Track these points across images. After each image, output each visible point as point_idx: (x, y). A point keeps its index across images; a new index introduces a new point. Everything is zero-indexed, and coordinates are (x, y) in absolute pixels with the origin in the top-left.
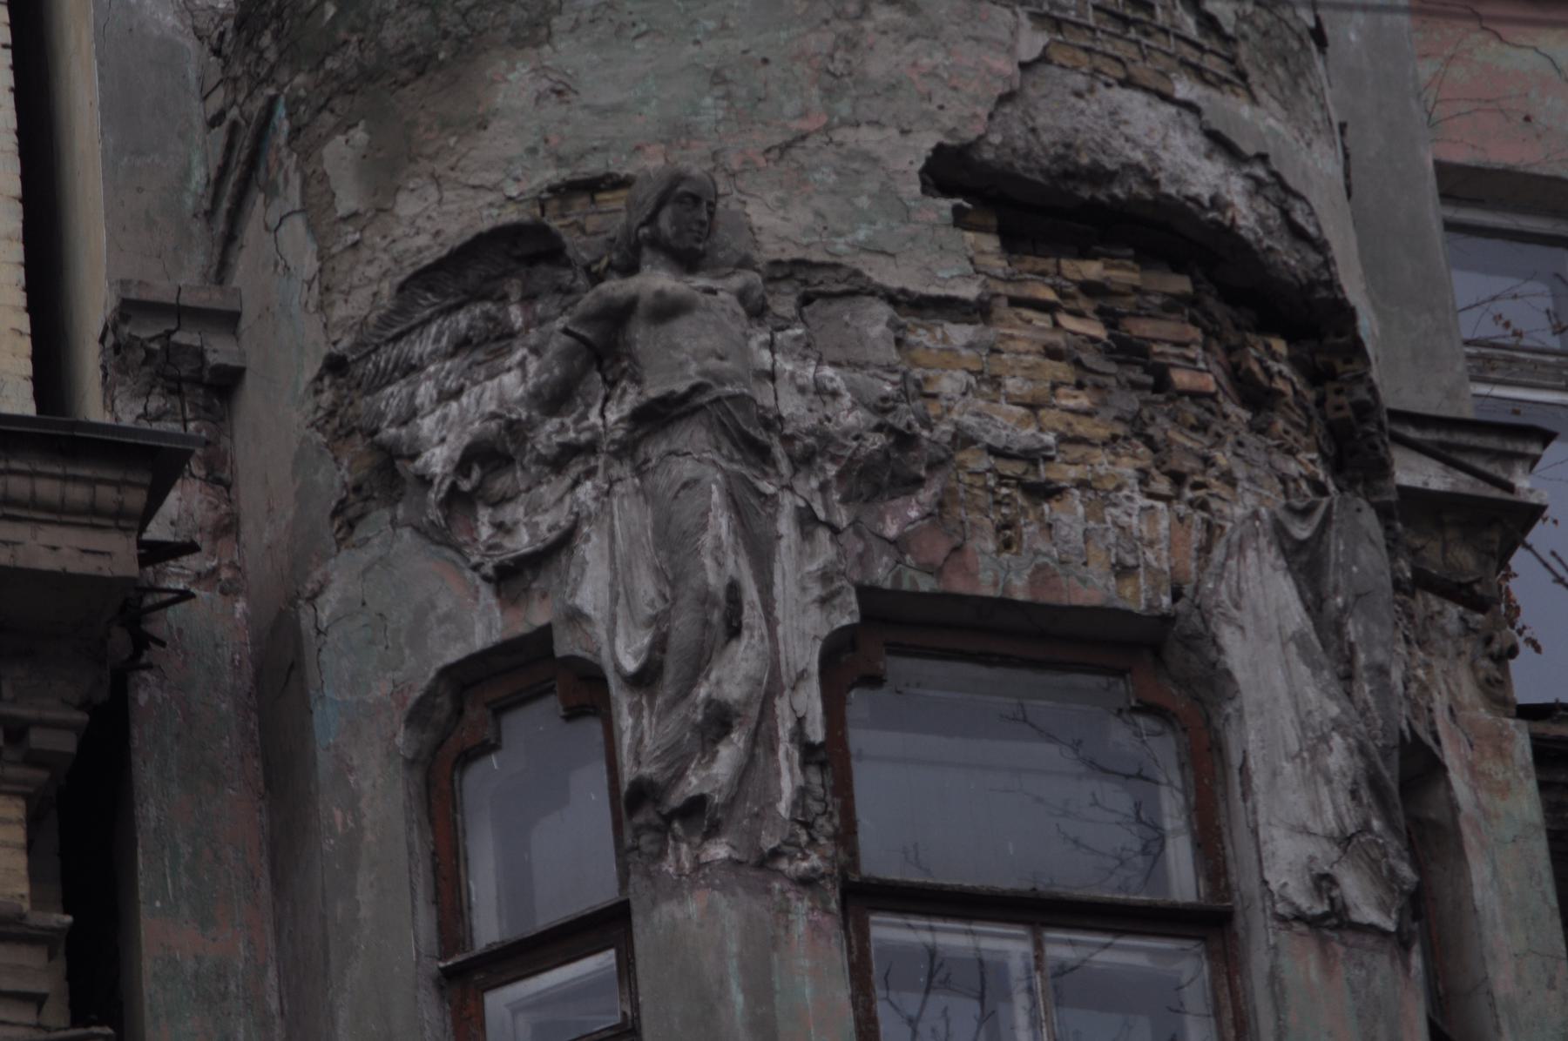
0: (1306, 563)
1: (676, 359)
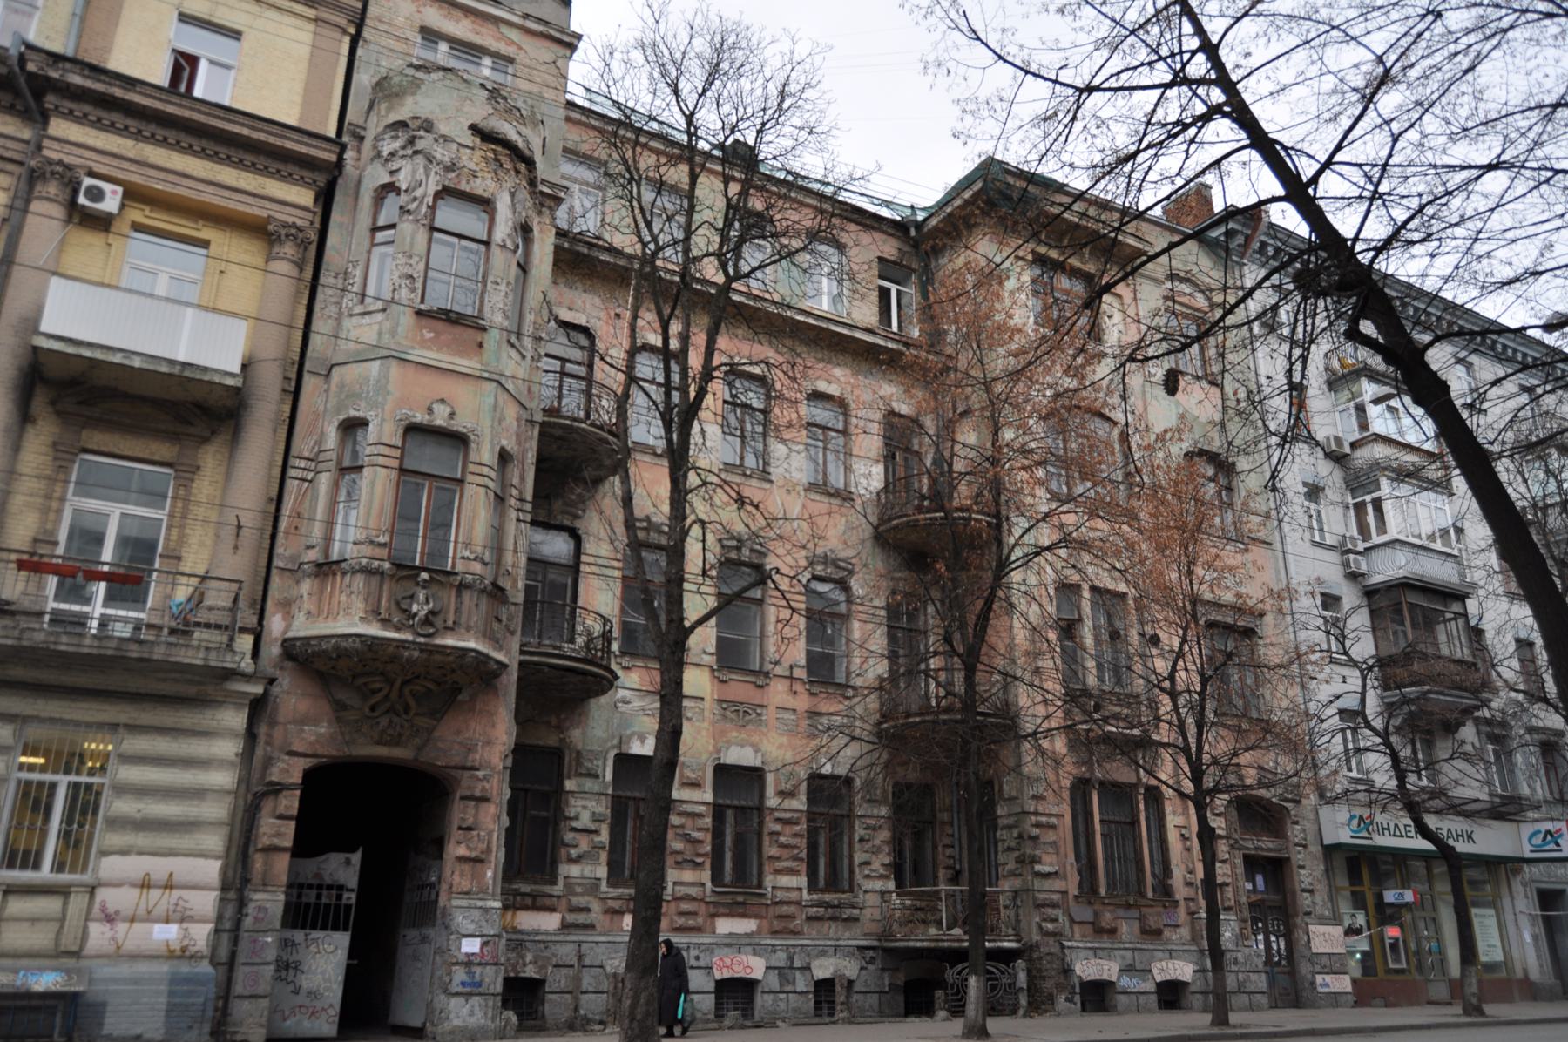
0: (513, 195)
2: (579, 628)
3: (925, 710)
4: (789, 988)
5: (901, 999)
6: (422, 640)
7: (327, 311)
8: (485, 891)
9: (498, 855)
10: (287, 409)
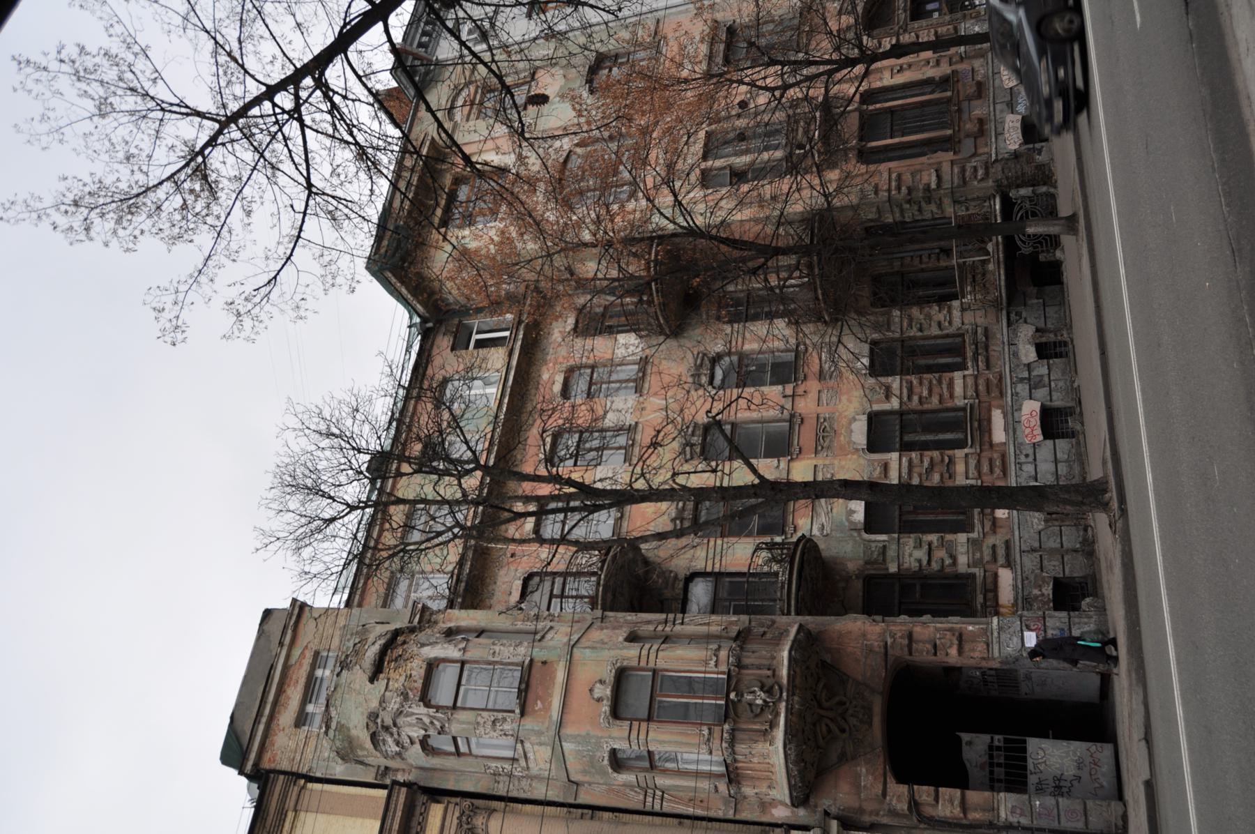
0: (423, 645)
1: (389, 722)
2: (766, 569)
3: (811, 286)
4: (1046, 379)
5: (1048, 289)
6: (785, 694)
7: (526, 788)
8: (985, 631)
9: (954, 622)
10: (606, 815)
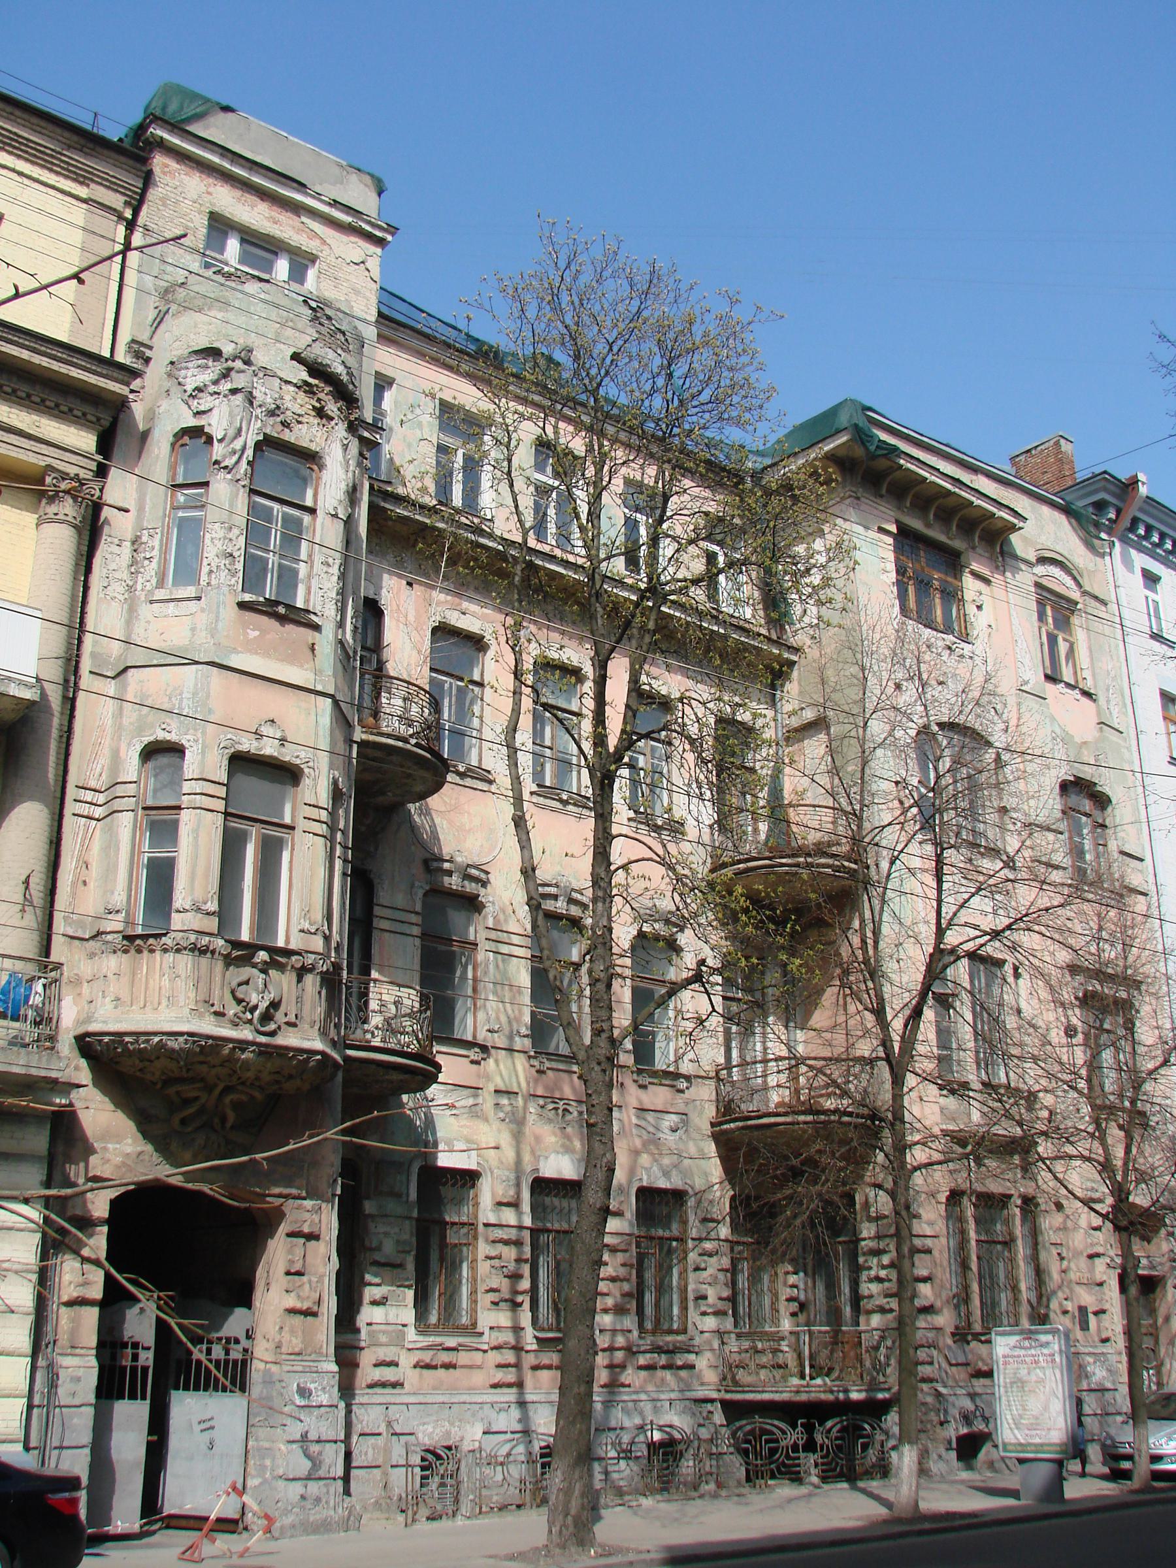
2: (373, 1005)
6: (263, 1039)
